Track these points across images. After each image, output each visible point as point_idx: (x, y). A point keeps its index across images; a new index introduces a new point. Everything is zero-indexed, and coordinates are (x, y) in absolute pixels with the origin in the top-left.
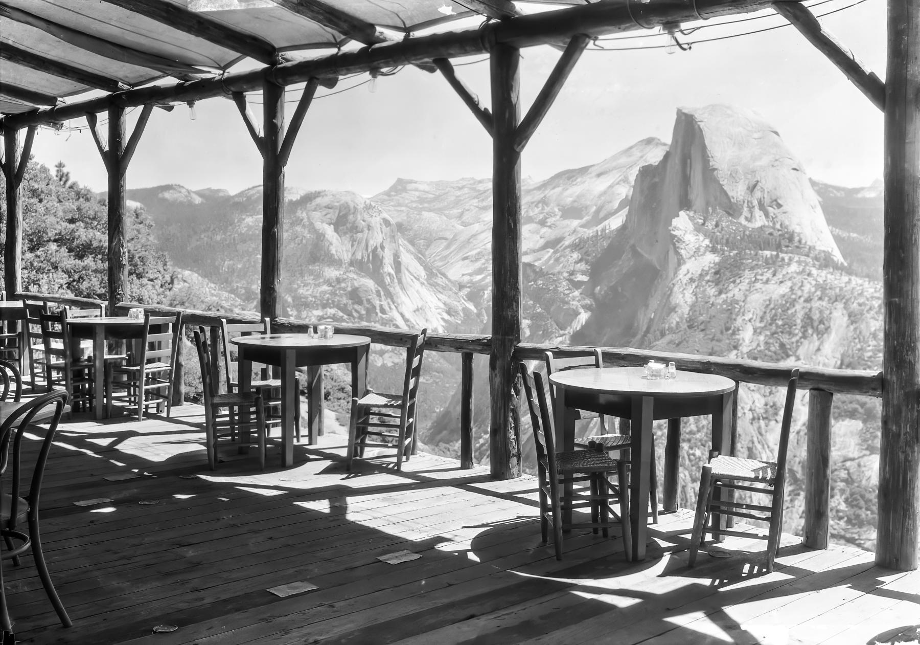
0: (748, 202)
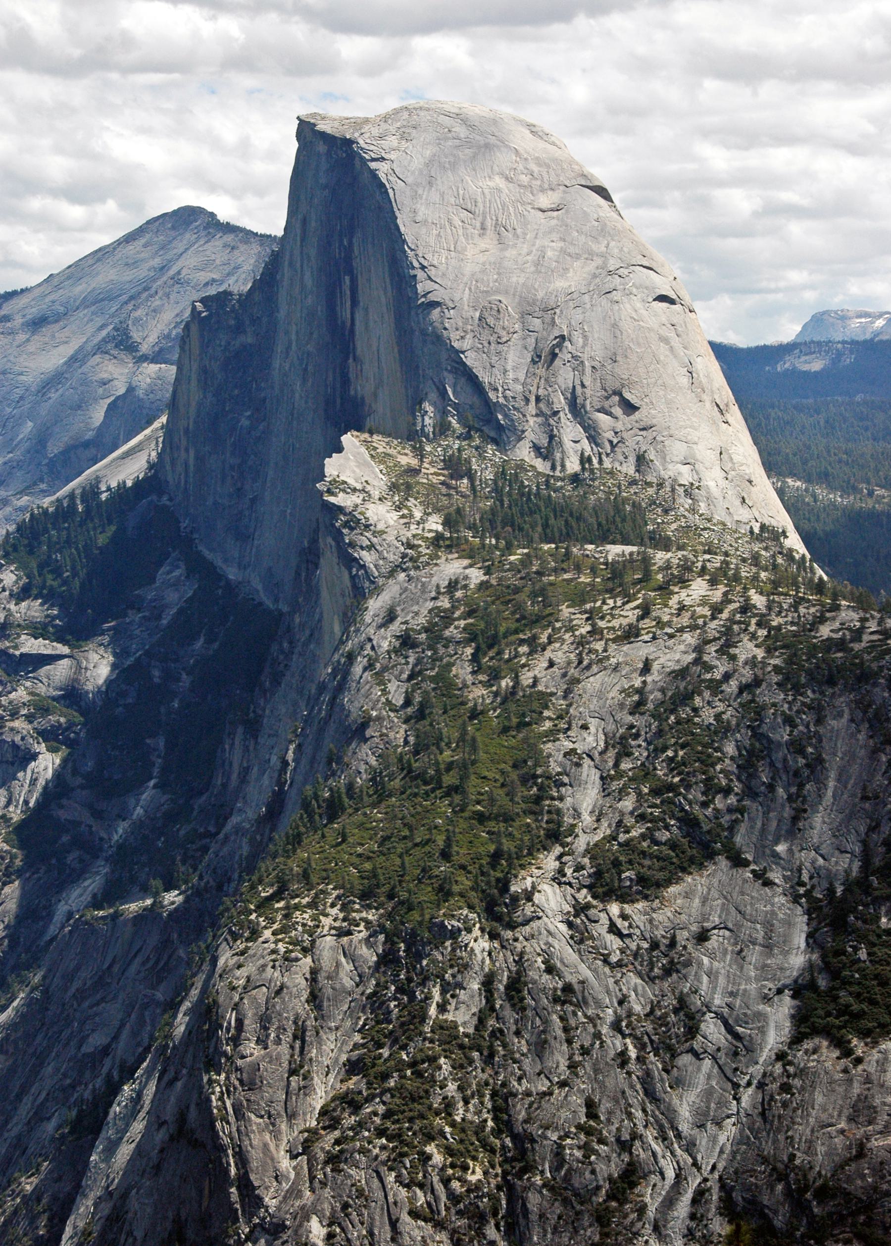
0: (538, 399)
